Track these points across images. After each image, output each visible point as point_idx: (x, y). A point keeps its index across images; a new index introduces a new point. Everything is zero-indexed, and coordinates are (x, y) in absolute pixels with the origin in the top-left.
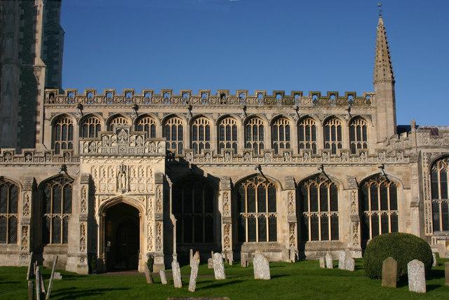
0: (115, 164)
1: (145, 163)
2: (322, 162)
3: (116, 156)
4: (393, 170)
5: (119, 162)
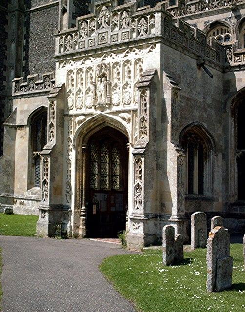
0: (94, 63)
1: (132, 56)
3: (96, 52)
5: (99, 60)
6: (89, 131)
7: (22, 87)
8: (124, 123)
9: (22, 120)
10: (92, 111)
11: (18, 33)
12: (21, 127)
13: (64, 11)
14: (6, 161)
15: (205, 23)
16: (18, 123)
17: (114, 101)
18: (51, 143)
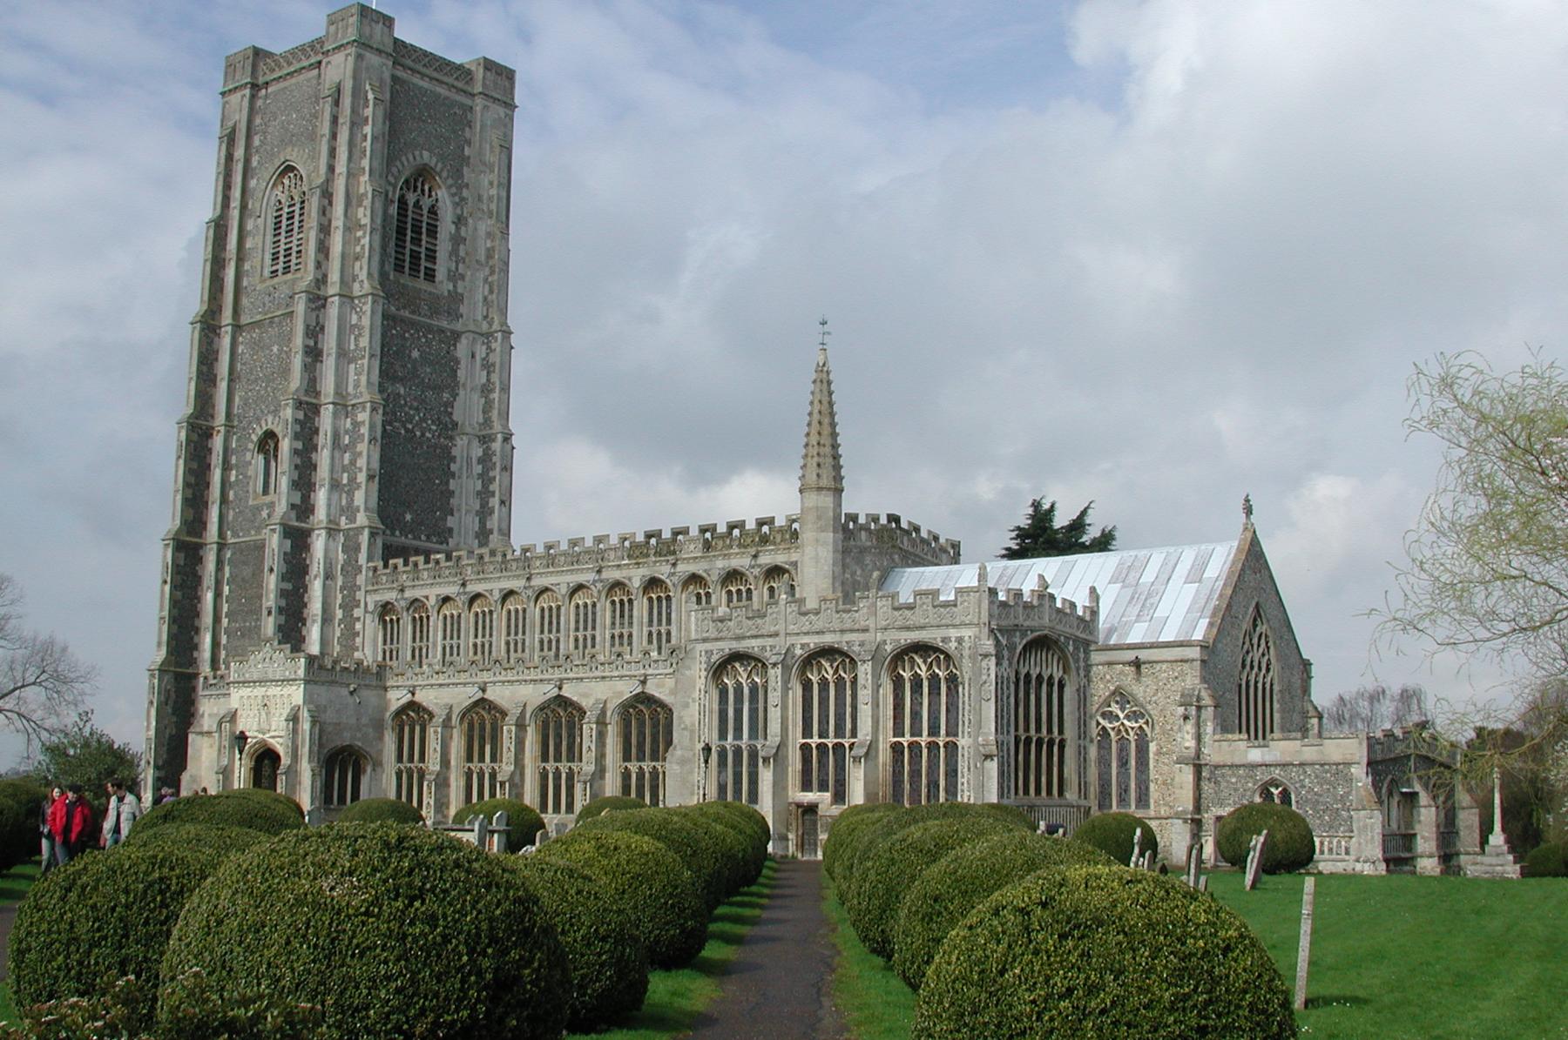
0: (259, 691)
2: (557, 676)
3: (261, 682)
4: (663, 686)
6: (256, 751)
7: (211, 685)
8: (278, 746)
9: (210, 726)
10: (256, 734)
12: (209, 733)
13: (271, 570)
14: (191, 776)
16: (206, 729)
17: (273, 728)
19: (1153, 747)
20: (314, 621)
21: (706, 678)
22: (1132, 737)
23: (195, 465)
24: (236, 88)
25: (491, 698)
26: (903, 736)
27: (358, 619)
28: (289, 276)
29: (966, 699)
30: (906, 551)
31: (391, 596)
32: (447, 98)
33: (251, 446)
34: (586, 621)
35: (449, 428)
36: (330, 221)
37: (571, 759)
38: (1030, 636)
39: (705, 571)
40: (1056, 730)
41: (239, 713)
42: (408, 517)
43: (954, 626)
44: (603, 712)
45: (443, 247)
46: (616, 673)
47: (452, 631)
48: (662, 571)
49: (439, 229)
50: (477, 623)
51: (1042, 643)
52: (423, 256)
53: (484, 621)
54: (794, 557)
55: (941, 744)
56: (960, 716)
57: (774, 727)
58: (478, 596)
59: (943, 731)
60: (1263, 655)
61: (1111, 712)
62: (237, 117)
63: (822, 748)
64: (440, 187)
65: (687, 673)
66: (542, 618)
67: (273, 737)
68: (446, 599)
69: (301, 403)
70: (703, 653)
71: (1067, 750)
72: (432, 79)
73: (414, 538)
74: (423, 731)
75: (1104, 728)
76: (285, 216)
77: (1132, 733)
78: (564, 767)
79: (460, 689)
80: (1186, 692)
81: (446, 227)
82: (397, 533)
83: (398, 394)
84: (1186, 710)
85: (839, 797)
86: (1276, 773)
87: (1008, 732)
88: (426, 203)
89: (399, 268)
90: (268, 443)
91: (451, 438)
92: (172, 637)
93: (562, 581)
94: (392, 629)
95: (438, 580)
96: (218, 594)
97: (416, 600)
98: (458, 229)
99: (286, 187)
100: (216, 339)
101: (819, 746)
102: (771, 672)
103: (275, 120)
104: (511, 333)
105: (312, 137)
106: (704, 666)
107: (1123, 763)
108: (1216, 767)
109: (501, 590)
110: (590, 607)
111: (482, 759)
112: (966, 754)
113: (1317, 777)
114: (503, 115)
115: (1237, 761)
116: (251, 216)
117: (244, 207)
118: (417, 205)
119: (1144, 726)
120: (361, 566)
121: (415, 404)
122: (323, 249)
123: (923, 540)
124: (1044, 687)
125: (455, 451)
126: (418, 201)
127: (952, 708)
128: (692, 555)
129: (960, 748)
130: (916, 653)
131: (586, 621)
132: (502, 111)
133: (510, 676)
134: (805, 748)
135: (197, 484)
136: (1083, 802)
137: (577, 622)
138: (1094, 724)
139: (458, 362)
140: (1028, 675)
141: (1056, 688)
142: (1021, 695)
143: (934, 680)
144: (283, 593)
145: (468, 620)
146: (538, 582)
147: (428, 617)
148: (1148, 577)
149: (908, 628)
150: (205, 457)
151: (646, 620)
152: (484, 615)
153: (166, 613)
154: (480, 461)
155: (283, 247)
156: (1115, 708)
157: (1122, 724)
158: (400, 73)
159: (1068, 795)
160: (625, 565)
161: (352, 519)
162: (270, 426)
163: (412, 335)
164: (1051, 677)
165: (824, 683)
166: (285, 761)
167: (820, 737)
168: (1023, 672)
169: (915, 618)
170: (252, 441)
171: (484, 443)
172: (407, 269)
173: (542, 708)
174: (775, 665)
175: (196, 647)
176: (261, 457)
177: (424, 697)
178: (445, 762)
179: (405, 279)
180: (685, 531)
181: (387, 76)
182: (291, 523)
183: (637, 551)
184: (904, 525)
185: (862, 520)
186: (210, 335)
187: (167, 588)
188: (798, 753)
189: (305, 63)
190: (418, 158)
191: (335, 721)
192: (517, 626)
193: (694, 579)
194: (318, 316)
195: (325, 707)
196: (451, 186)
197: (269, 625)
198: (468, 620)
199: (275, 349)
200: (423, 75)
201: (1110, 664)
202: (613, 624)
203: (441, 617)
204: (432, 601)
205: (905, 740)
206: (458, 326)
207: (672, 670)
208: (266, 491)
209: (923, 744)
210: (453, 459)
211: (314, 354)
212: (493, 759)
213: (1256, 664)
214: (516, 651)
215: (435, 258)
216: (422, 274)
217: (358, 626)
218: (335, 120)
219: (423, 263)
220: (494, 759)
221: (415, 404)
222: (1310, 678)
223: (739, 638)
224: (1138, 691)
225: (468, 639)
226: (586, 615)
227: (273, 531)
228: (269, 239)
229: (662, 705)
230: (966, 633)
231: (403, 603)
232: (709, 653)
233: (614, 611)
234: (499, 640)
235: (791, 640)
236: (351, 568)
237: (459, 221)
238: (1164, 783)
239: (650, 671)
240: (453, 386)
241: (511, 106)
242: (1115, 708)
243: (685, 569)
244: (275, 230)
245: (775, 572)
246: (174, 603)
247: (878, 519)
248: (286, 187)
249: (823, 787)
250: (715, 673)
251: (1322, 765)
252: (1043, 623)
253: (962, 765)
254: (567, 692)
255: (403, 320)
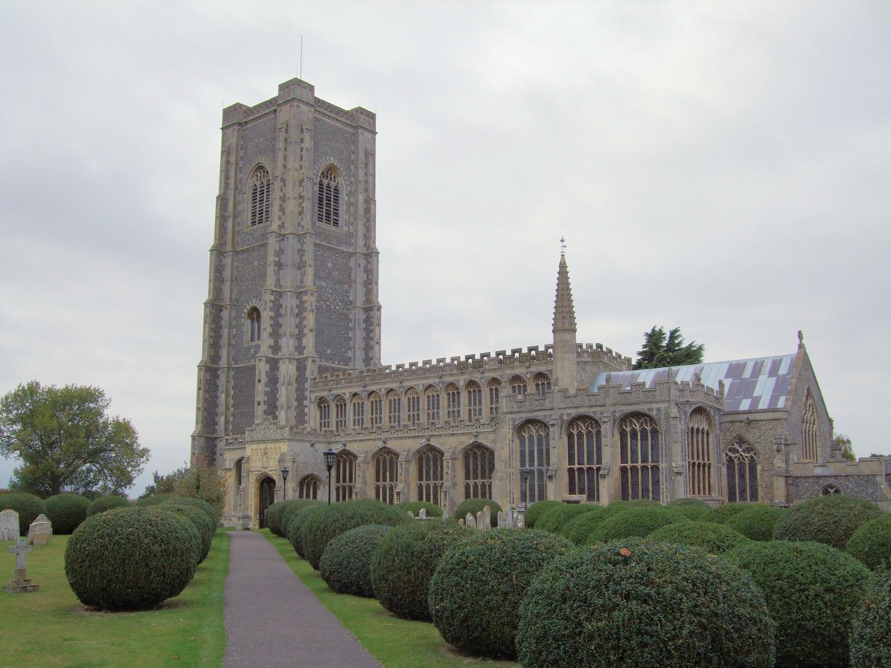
0: (263, 446)
3: (263, 441)
7: (230, 443)
8: (274, 476)
11: (227, 386)
12: (229, 469)
15: (350, 393)
16: (227, 467)
18: (243, 486)
19: (759, 467)
20: (282, 408)
21: (513, 433)
22: (747, 461)
23: (214, 326)
24: (229, 126)
25: (390, 447)
26: (627, 463)
27: (306, 406)
28: (262, 225)
29: (663, 442)
30: (606, 364)
31: (324, 394)
32: (342, 129)
33: (244, 315)
34: (433, 404)
35: (349, 304)
36: (285, 194)
37: (435, 478)
38: (694, 407)
39: (500, 376)
40: (706, 458)
41: (251, 458)
42: (329, 352)
43: (656, 402)
44: (454, 453)
45: (342, 208)
46: (460, 432)
47: (359, 411)
48: (476, 377)
49: (339, 199)
50: (372, 407)
51: (699, 411)
52: (332, 213)
53: (376, 406)
54: (550, 367)
55: (649, 467)
56: (660, 452)
57: (553, 459)
58: (373, 392)
59: (650, 460)
60: (811, 416)
61: (734, 449)
62: (231, 141)
63: (580, 470)
64: (340, 176)
65: (503, 430)
66: (409, 403)
67: (271, 471)
68: (355, 394)
69: (273, 291)
70: (510, 420)
71: (712, 469)
72: (334, 118)
73: (332, 363)
74: (351, 465)
75: (730, 457)
76: (258, 193)
77: (746, 460)
78: (431, 483)
79: (371, 442)
80: (777, 436)
81: (343, 198)
82: (323, 360)
83: (322, 286)
84: (778, 446)
85: (593, 495)
86: (832, 481)
87: (685, 460)
88: (333, 184)
89: (320, 219)
90: (255, 314)
91: (349, 309)
92: (205, 418)
93: (420, 384)
94: (325, 411)
95: (350, 384)
96: (227, 395)
97: (339, 395)
98: (349, 198)
99: (259, 178)
100: (223, 259)
101: (579, 469)
102: (603, 426)
103: (251, 142)
104: (379, 253)
105: (273, 150)
106: (511, 427)
107: (742, 476)
108: (796, 477)
109: (386, 389)
110: (435, 397)
111: (385, 480)
112: (664, 472)
113: (855, 483)
114: (370, 137)
115: (808, 475)
116: (239, 193)
117: (236, 188)
118: (328, 186)
119: (754, 456)
120: (307, 378)
121: (331, 291)
122: (282, 210)
123: (614, 358)
124: (700, 434)
125: (351, 317)
126: (329, 184)
127: (655, 447)
128: (493, 367)
129: (660, 469)
130: (633, 418)
131: (433, 404)
132: (369, 135)
133: (400, 435)
134: (571, 471)
135: (215, 336)
136: (720, 498)
137: (429, 405)
138: (724, 455)
139: (351, 269)
140: (692, 428)
141: (705, 435)
142: (690, 438)
143: (644, 431)
144: (266, 393)
145: (367, 405)
146: (407, 384)
147: (345, 404)
148: (747, 374)
149: (629, 404)
150: (219, 322)
151: (467, 403)
152: (376, 402)
153: (200, 406)
154: (365, 321)
155: (258, 209)
156: (736, 446)
157: (741, 455)
158: (317, 116)
159: (713, 494)
160: (455, 374)
161: (301, 353)
162: (254, 305)
163: (328, 255)
164: (703, 429)
165: (580, 435)
166: (279, 483)
167: (579, 464)
168: (691, 426)
169: (633, 398)
170: (245, 313)
171: (366, 312)
172: (324, 220)
173: (418, 451)
174: (553, 425)
175: (216, 423)
176: (249, 321)
177: (352, 447)
178: (365, 482)
179: (323, 225)
180: (488, 355)
181: (311, 117)
182: (269, 356)
183: (461, 366)
184: (604, 349)
185: (584, 347)
186: (221, 257)
187: (201, 392)
188: (567, 473)
189: (267, 111)
190: (328, 160)
191: (304, 461)
192: (395, 408)
193: (495, 381)
194: (280, 245)
195: (299, 453)
196: (345, 175)
197: (259, 410)
198: (367, 405)
199: (256, 263)
200: (329, 117)
201: (733, 422)
202: (449, 406)
203: (352, 404)
204: (347, 396)
205: (629, 465)
206: (351, 250)
207: (492, 429)
208: (252, 340)
209: (639, 467)
210: (350, 320)
211: (279, 265)
212: (391, 480)
213: (808, 421)
214: (376, 423)
215: (338, 214)
216: (332, 223)
217: (306, 410)
218: (286, 140)
219: (332, 217)
220: (391, 480)
221: (331, 291)
222: (832, 428)
223: (530, 412)
224: (750, 437)
225: (367, 416)
226: (433, 401)
227: (260, 360)
228: (250, 205)
229: (487, 449)
230: (662, 406)
231: (331, 397)
232: (514, 420)
233: (449, 399)
234: (385, 415)
235: (562, 411)
236: (301, 378)
237: (350, 194)
238: (766, 486)
239: (480, 430)
240: (349, 281)
241: (374, 133)
242: (736, 446)
243: (490, 375)
244: (253, 200)
245: (540, 375)
246: (205, 400)
247: (582, 346)
248: (259, 178)
249: (582, 492)
250: (517, 430)
251: (859, 476)
252: (698, 399)
253: (662, 478)
254: (434, 442)
255: (323, 246)
